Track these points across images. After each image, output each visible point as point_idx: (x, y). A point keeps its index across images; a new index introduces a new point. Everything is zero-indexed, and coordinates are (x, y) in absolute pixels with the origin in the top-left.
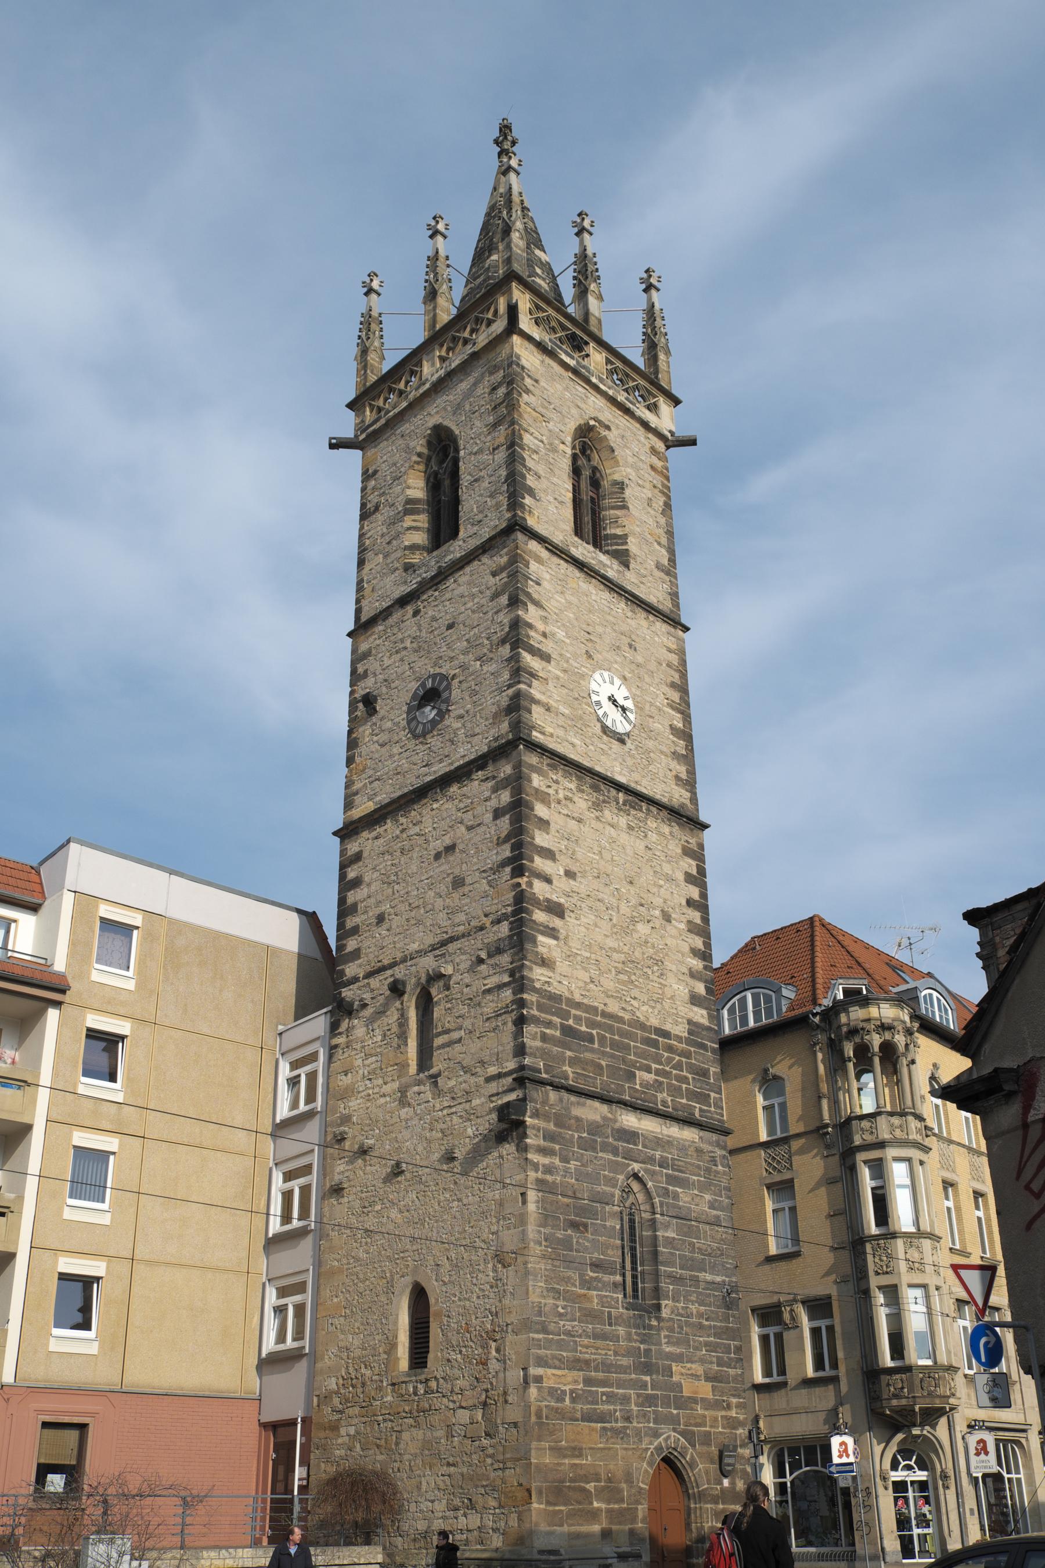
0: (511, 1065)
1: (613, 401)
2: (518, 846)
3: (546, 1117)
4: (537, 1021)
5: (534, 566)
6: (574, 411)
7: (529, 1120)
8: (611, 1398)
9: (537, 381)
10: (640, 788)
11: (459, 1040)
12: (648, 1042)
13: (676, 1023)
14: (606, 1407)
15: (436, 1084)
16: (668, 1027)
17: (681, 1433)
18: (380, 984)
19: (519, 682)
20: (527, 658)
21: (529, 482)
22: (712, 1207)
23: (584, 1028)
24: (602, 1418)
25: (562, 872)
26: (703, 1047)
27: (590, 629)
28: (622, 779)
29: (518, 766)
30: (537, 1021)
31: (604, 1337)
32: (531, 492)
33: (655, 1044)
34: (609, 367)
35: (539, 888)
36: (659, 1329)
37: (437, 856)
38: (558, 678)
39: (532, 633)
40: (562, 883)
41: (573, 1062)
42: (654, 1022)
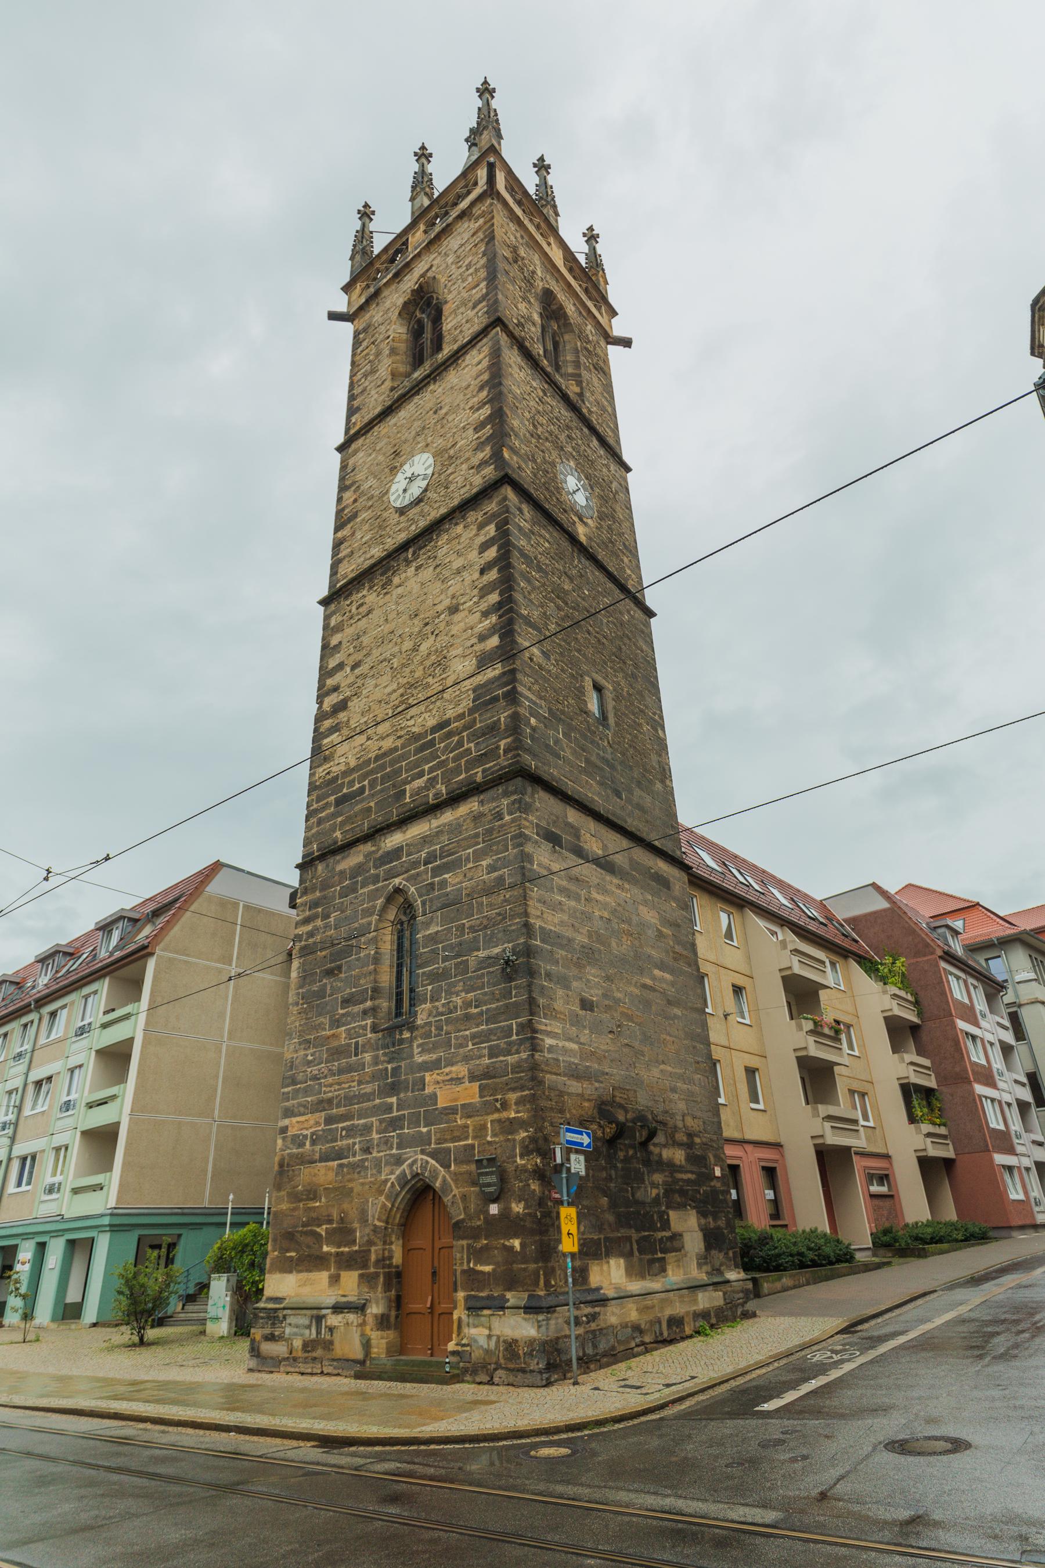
8: (351, 1131)
14: (345, 1142)
24: (339, 1155)
31: (350, 1069)
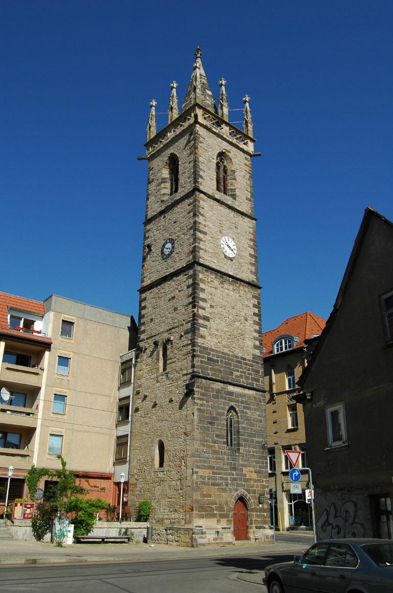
0: (190, 371)
1: (231, 143)
2: (194, 298)
3: (202, 388)
4: (199, 356)
5: (202, 202)
6: (218, 147)
7: (195, 389)
8: (221, 478)
9: (204, 139)
10: (238, 277)
11: (175, 362)
12: (238, 362)
13: (248, 355)
14: (220, 481)
15: (167, 376)
16: (245, 357)
17: (246, 490)
18: (151, 341)
19: (196, 243)
20: (199, 235)
21: (200, 174)
22: (259, 416)
23: (215, 358)
24: (218, 485)
25: (209, 306)
26: (258, 363)
27: (221, 222)
28: (231, 273)
29: (194, 271)
30: (199, 356)
32: (202, 177)
33: (240, 362)
34: (230, 131)
35: (201, 312)
36: (239, 456)
37: (169, 300)
38: (209, 240)
39: (201, 226)
40: (209, 310)
41: (211, 369)
42: (240, 355)
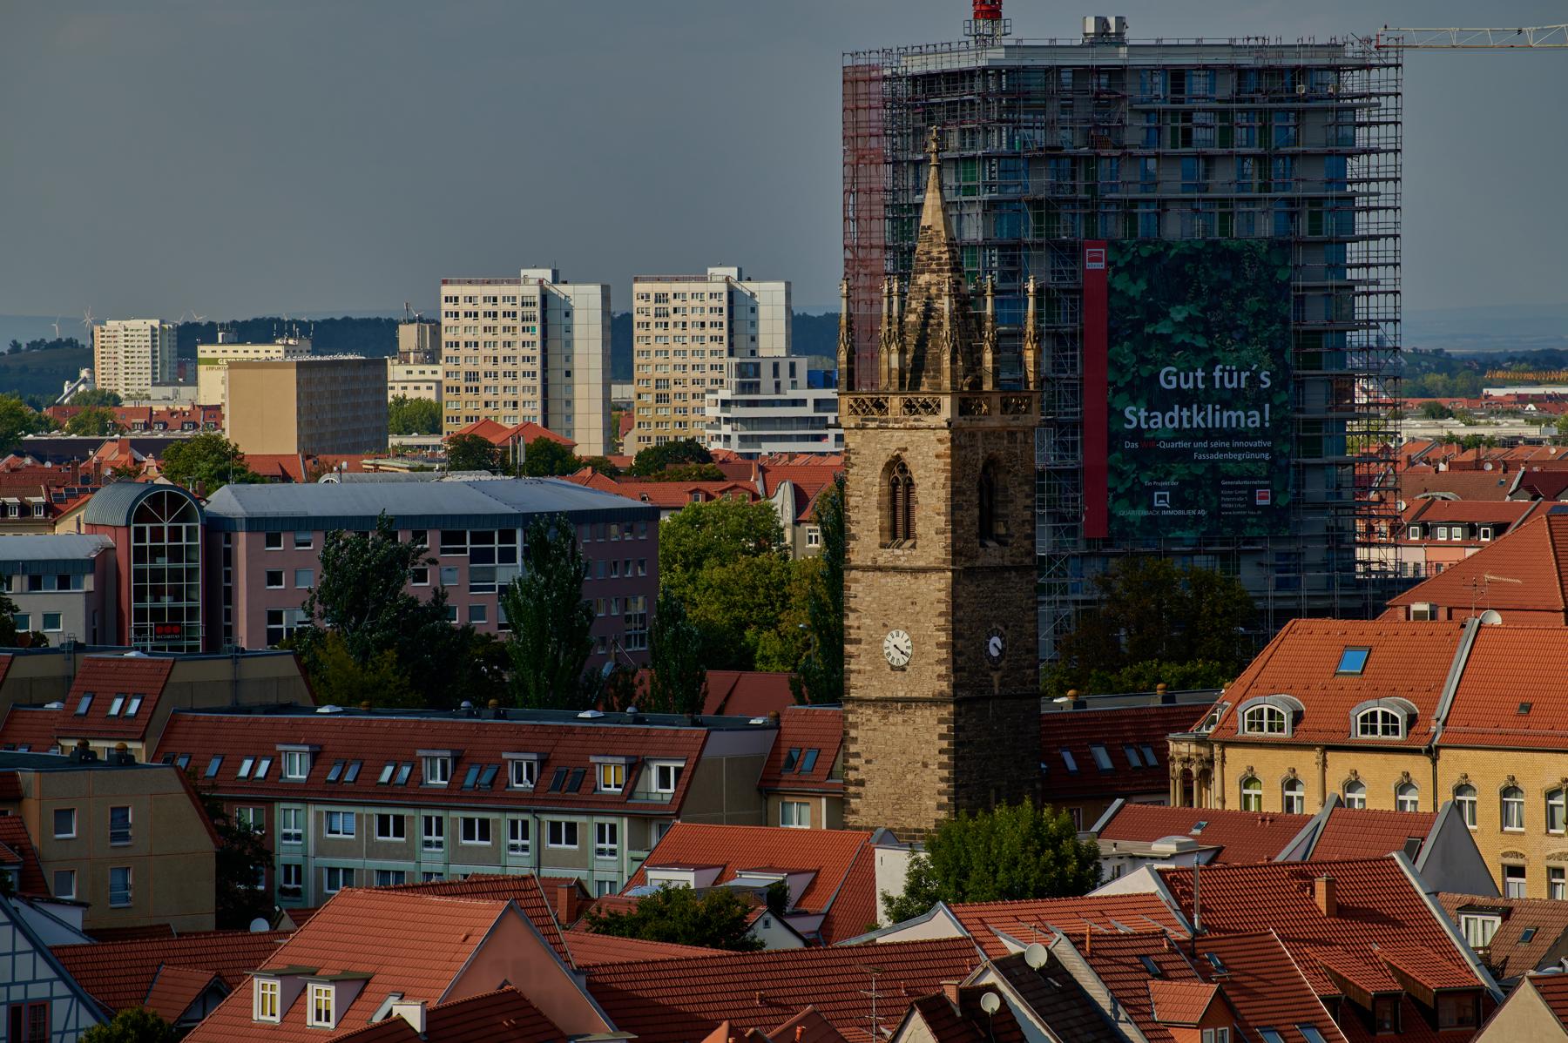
5: (853, 586)
28: (901, 694)
32: (853, 537)
42: (915, 826)
